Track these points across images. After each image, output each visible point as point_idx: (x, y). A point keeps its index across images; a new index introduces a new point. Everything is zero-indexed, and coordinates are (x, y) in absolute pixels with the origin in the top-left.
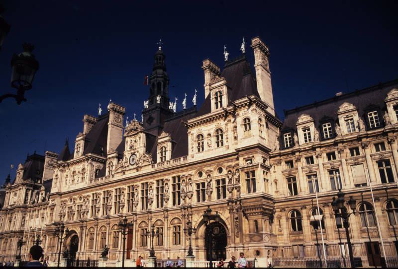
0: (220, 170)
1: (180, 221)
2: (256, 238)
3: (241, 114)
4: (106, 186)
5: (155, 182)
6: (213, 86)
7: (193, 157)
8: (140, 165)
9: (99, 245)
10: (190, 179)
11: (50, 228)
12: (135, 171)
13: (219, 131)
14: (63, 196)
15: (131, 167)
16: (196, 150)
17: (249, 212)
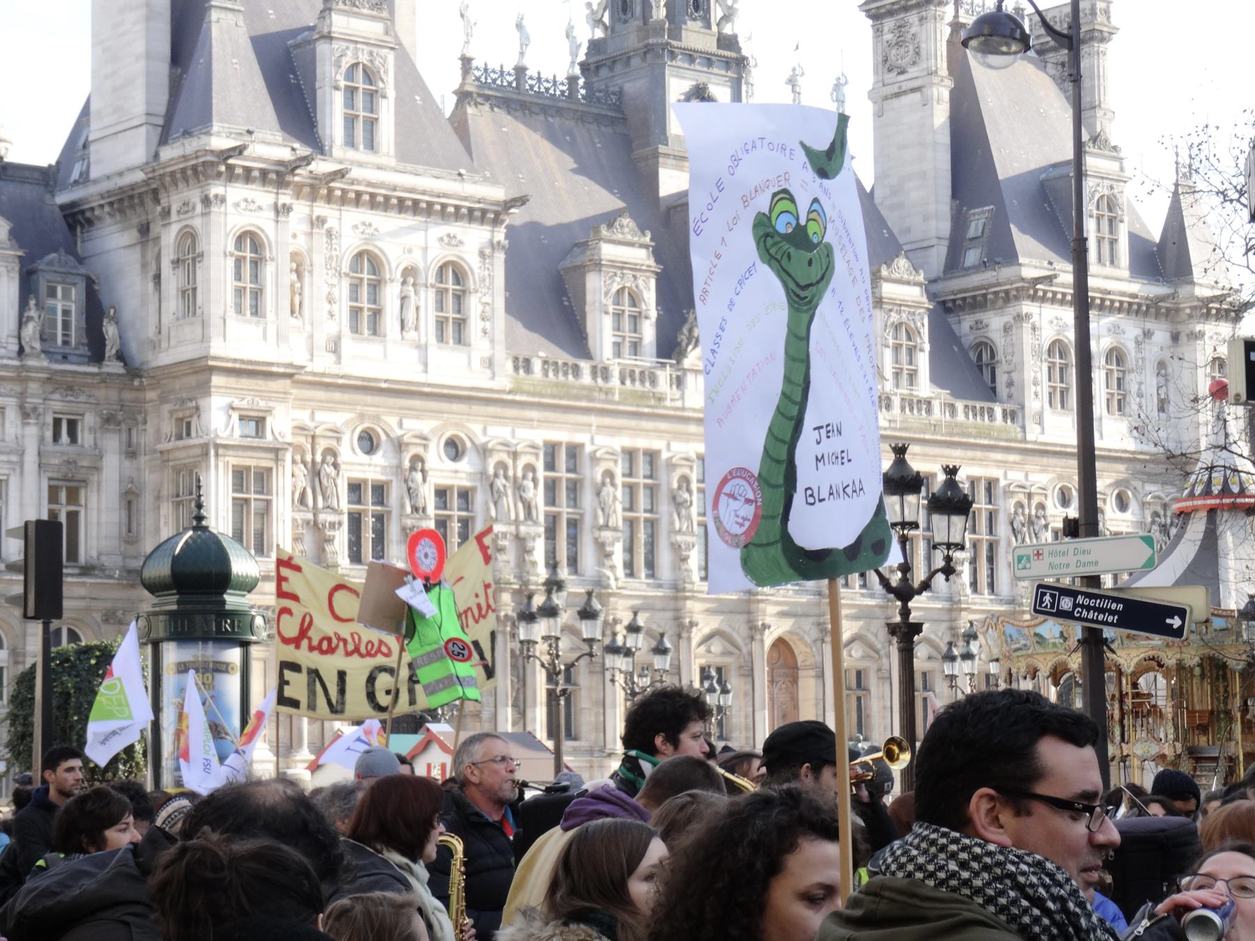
7: (1040, 423)
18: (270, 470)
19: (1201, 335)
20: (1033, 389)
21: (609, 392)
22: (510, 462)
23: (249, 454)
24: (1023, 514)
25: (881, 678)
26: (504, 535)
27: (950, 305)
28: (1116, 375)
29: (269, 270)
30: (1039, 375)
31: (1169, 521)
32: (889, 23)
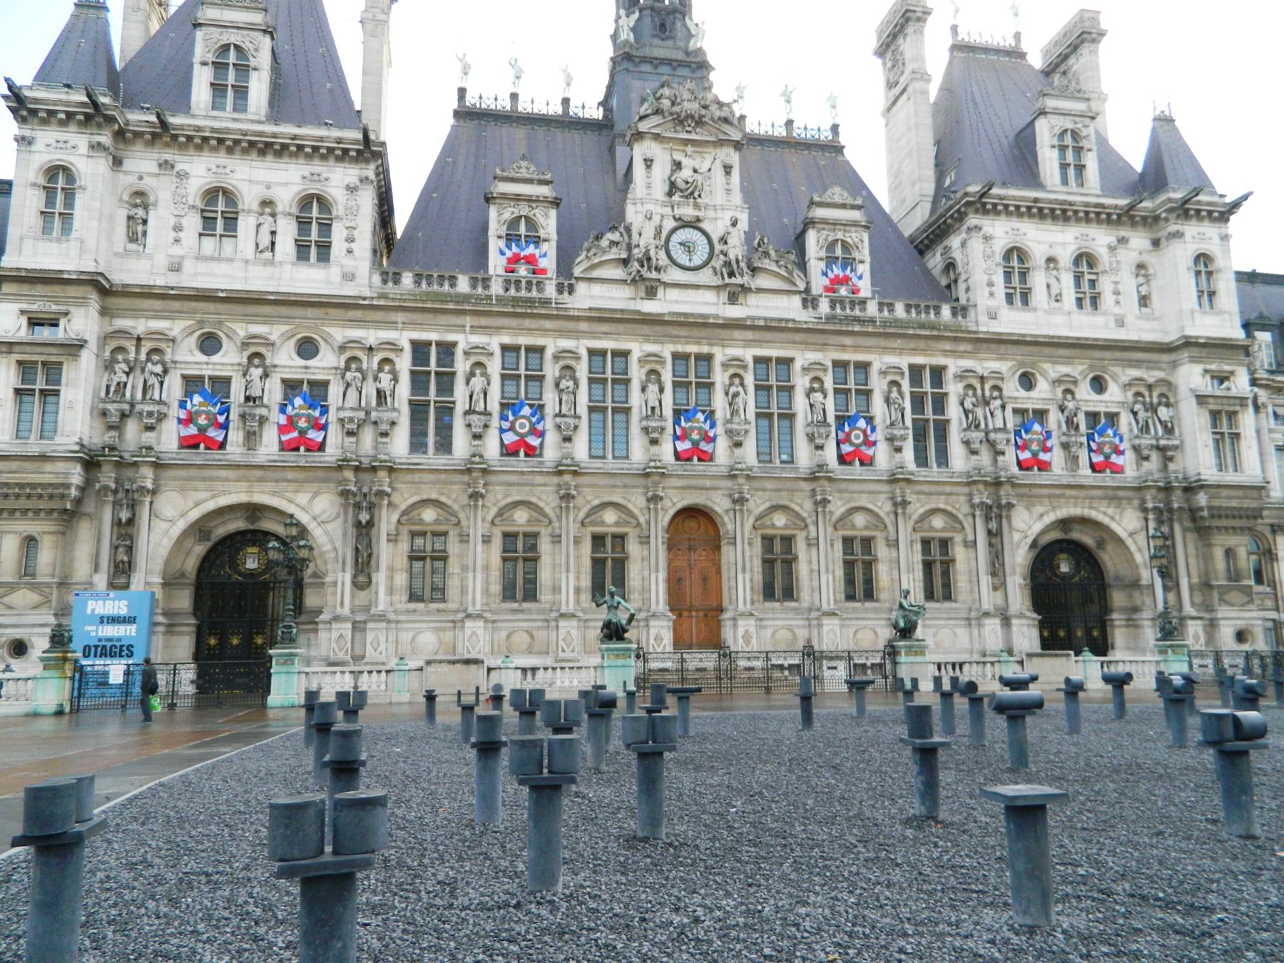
0: (1099, 385)
1: (961, 523)
2: (1235, 596)
3: (1188, 237)
4: (527, 323)
5: (830, 365)
6: (1051, 103)
7: (993, 316)
8: (745, 280)
9: (496, 588)
10: (996, 388)
11: (46, 479)
12: (710, 296)
13: (1085, 259)
14: (113, 302)
15: (675, 275)
16: (1000, 290)
17: (1216, 523)
18: (61, 363)
19: (1178, 235)
20: (987, 290)
21: (489, 297)
22: (364, 358)
23: (38, 349)
24: (975, 395)
25: (809, 545)
26: (351, 420)
27: (926, 242)
28: (1087, 277)
29: (80, 200)
30: (994, 278)
31: (1155, 400)
32: (889, 55)
